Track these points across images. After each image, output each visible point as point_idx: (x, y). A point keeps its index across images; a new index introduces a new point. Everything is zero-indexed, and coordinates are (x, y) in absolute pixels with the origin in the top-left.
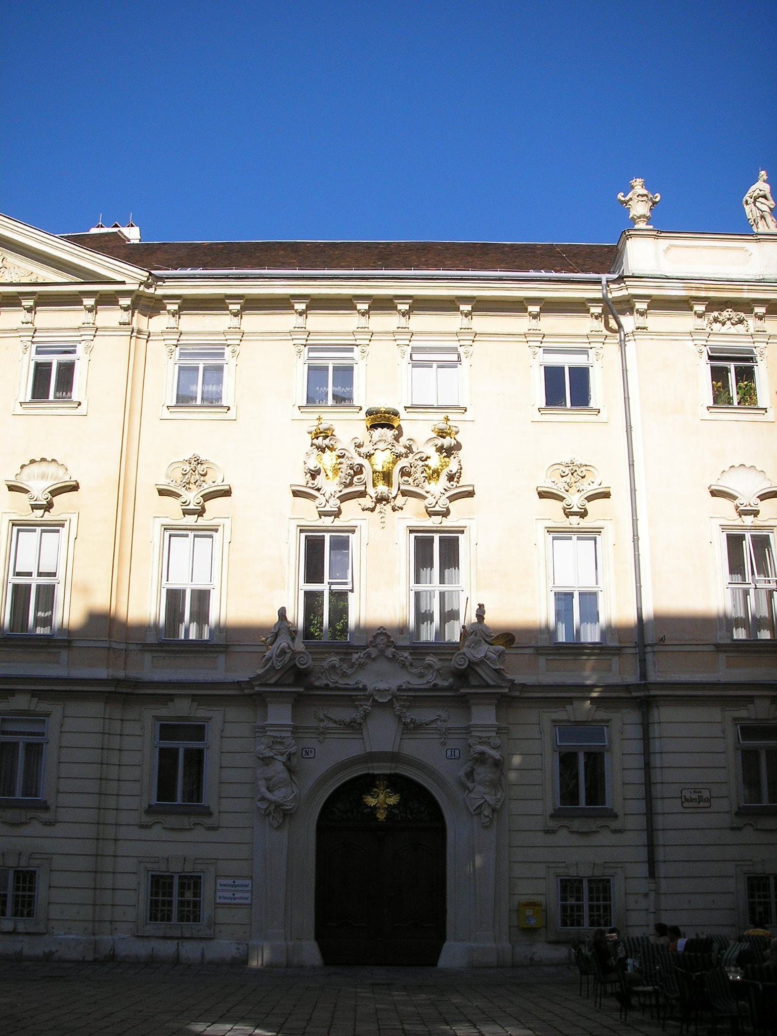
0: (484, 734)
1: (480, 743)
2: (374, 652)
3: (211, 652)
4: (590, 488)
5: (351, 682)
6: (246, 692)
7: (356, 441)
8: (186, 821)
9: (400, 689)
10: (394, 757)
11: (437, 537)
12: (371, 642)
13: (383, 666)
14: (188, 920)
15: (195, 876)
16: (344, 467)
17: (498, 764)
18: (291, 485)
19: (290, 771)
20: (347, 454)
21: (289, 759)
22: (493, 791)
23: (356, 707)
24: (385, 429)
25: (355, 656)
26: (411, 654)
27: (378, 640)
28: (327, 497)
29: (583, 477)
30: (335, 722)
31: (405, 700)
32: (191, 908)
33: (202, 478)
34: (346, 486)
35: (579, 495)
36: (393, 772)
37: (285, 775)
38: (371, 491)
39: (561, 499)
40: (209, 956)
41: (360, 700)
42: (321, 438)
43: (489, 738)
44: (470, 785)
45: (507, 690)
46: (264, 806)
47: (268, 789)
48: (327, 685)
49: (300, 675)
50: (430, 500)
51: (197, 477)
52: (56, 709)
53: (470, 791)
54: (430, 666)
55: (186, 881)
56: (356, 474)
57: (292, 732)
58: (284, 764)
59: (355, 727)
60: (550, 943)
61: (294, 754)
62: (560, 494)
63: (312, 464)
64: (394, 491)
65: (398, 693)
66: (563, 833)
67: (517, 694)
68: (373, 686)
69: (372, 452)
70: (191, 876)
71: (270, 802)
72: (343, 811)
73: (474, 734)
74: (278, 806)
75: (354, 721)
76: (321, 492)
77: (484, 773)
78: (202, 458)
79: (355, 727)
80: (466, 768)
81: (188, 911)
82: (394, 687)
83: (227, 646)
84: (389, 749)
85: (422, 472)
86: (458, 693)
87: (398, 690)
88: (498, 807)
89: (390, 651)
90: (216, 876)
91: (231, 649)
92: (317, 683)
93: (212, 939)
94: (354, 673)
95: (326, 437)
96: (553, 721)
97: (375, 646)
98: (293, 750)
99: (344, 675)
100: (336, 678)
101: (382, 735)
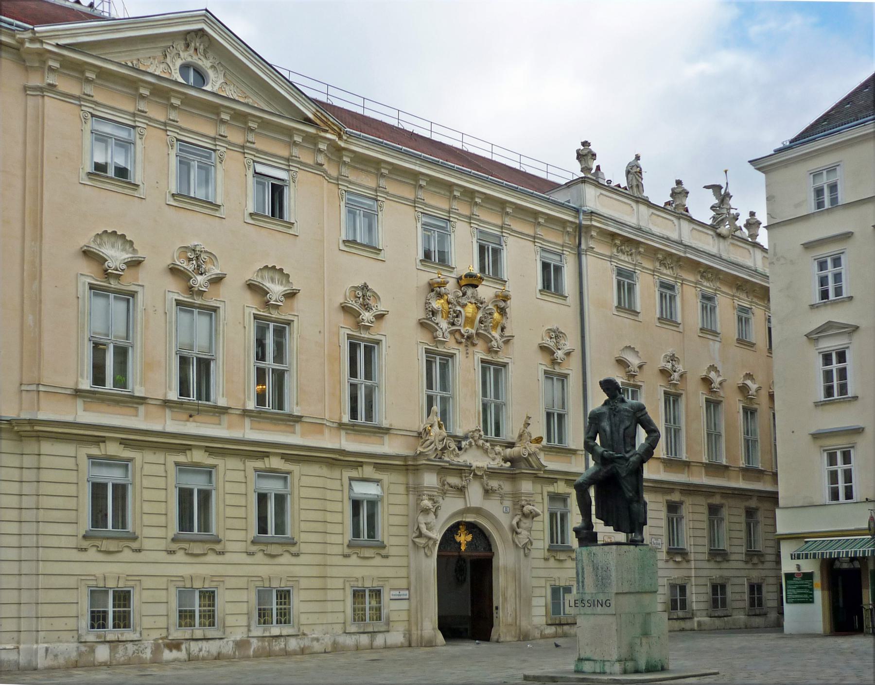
10: (478, 511)
44: (519, 530)
52: (295, 468)
59: (461, 490)
79: (461, 490)
84: (478, 506)
91: (391, 431)
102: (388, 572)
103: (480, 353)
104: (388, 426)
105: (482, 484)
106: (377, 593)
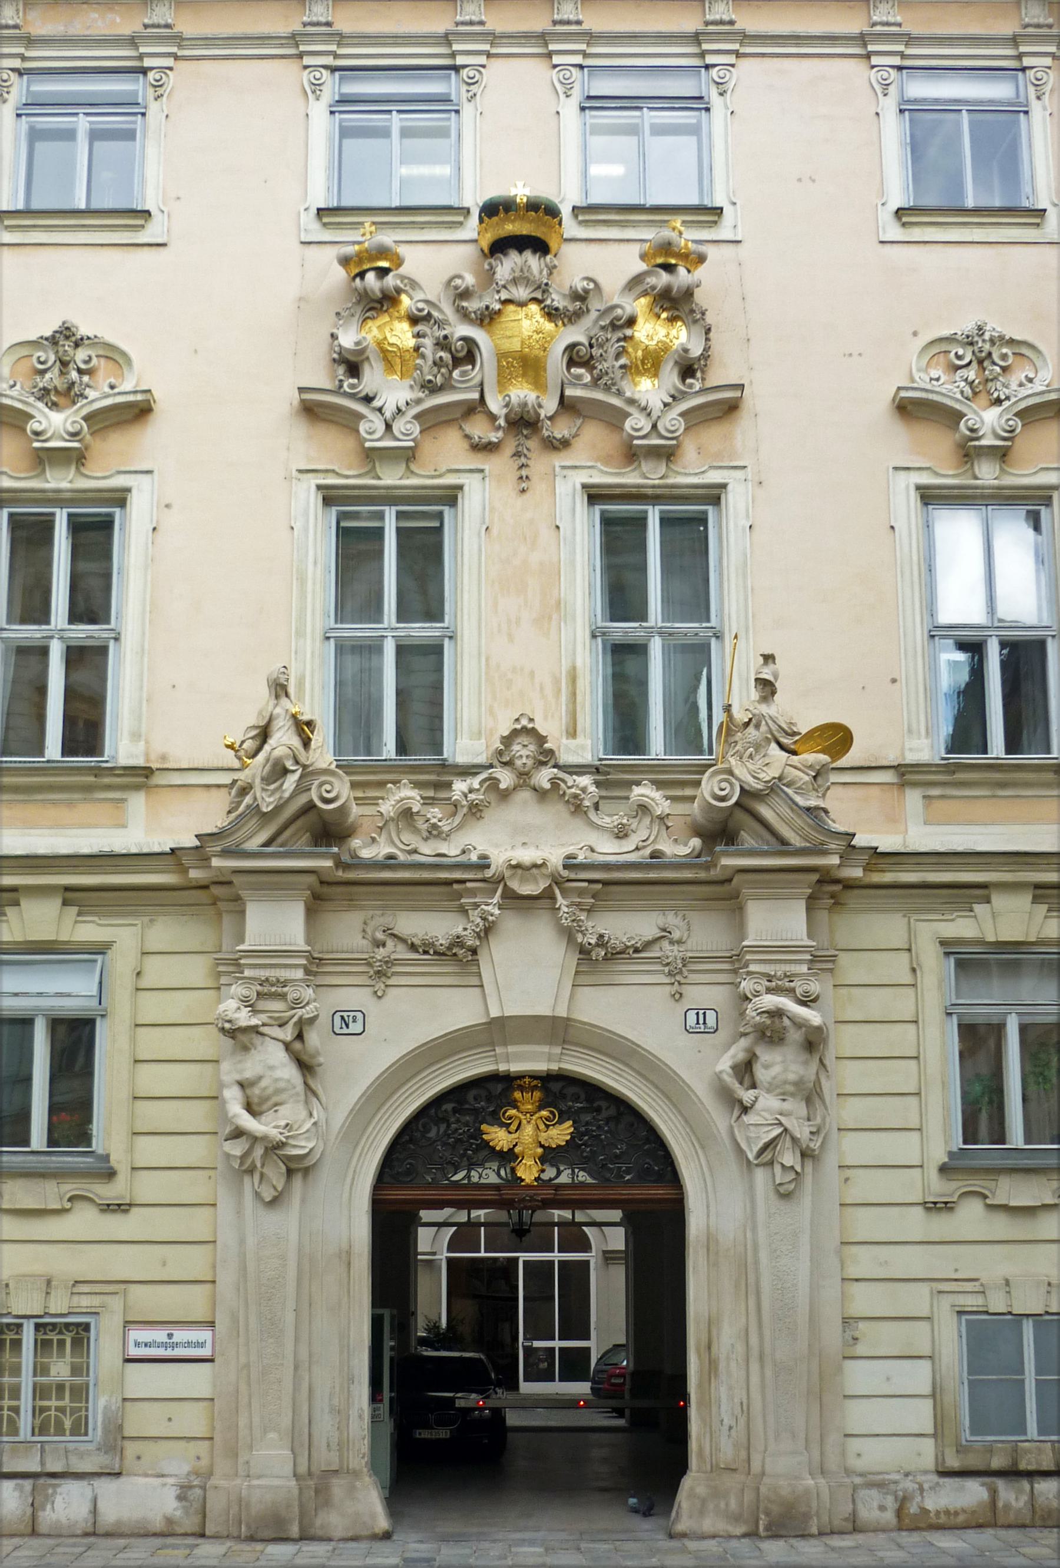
0: (780, 969)
1: (769, 991)
2: (506, 778)
3: (109, 787)
4: (1023, 392)
5: (451, 849)
6: (193, 874)
7: (458, 282)
8: (51, 1193)
9: (570, 863)
11: (654, 516)
12: (500, 753)
13: (523, 810)
14: (60, 1430)
15: (78, 1325)
16: (428, 342)
17: (813, 1042)
18: (301, 390)
19: (305, 1066)
20: (435, 314)
21: (300, 1037)
22: (802, 1109)
23: (463, 911)
24: (528, 254)
25: (460, 786)
26: (598, 784)
27: (516, 747)
28: (388, 415)
29: (1004, 369)
30: (413, 947)
31: (581, 893)
32: (66, 1402)
33: (86, 378)
34: (430, 387)
35: (996, 410)
36: (554, 1067)
37: (289, 1072)
38: (495, 404)
39: (954, 417)
40: (111, 1513)
41: (473, 893)
42: (370, 276)
43: (790, 977)
44: (747, 1096)
45: (835, 860)
46: (236, 1149)
47: (249, 1108)
48: (391, 857)
49: (328, 830)
50: (636, 423)
51: (74, 375)
53: (745, 1110)
54: (643, 809)
55: (54, 1337)
56: (457, 362)
57: (308, 972)
58: (287, 1046)
59: (461, 958)
60: (946, 1474)
61: (312, 1020)
62: (957, 406)
63: (348, 340)
64: (550, 405)
65: (565, 873)
66: (973, 1209)
67: (857, 873)
68: (509, 854)
69: (497, 306)
70: (67, 1325)
71: (255, 1139)
72: (436, 1142)
73: (753, 968)
74: (274, 1148)
75: (458, 942)
76: (377, 403)
77: (777, 1065)
78: (84, 330)
79: (461, 958)
80: (737, 1052)
81: (61, 1410)
82: (555, 857)
83: (147, 772)
84: (543, 1009)
85: (618, 356)
86: (715, 873)
87: (566, 867)
88: (815, 1145)
89: (543, 777)
90: (127, 1323)
91: (158, 779)
92: (366, 853)
93: (118, 1474)
94: (460, 827)
95: (383, 272)
96: (943, 943)
97: (508, 764)
98: (307, 1013)
99: (434, 832)
100: (410, 839)
101: (527, 974)
102: (124, 1263)
103: (587, 462)
104: (140, 762)
105: (569, 934)
106: (79, 1334)
